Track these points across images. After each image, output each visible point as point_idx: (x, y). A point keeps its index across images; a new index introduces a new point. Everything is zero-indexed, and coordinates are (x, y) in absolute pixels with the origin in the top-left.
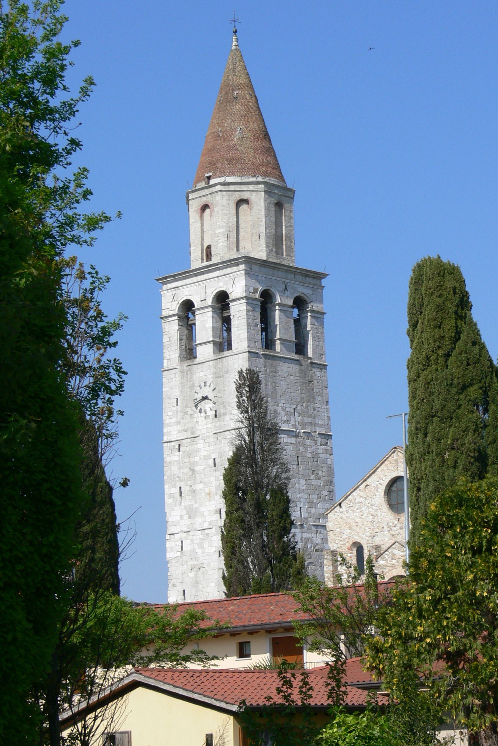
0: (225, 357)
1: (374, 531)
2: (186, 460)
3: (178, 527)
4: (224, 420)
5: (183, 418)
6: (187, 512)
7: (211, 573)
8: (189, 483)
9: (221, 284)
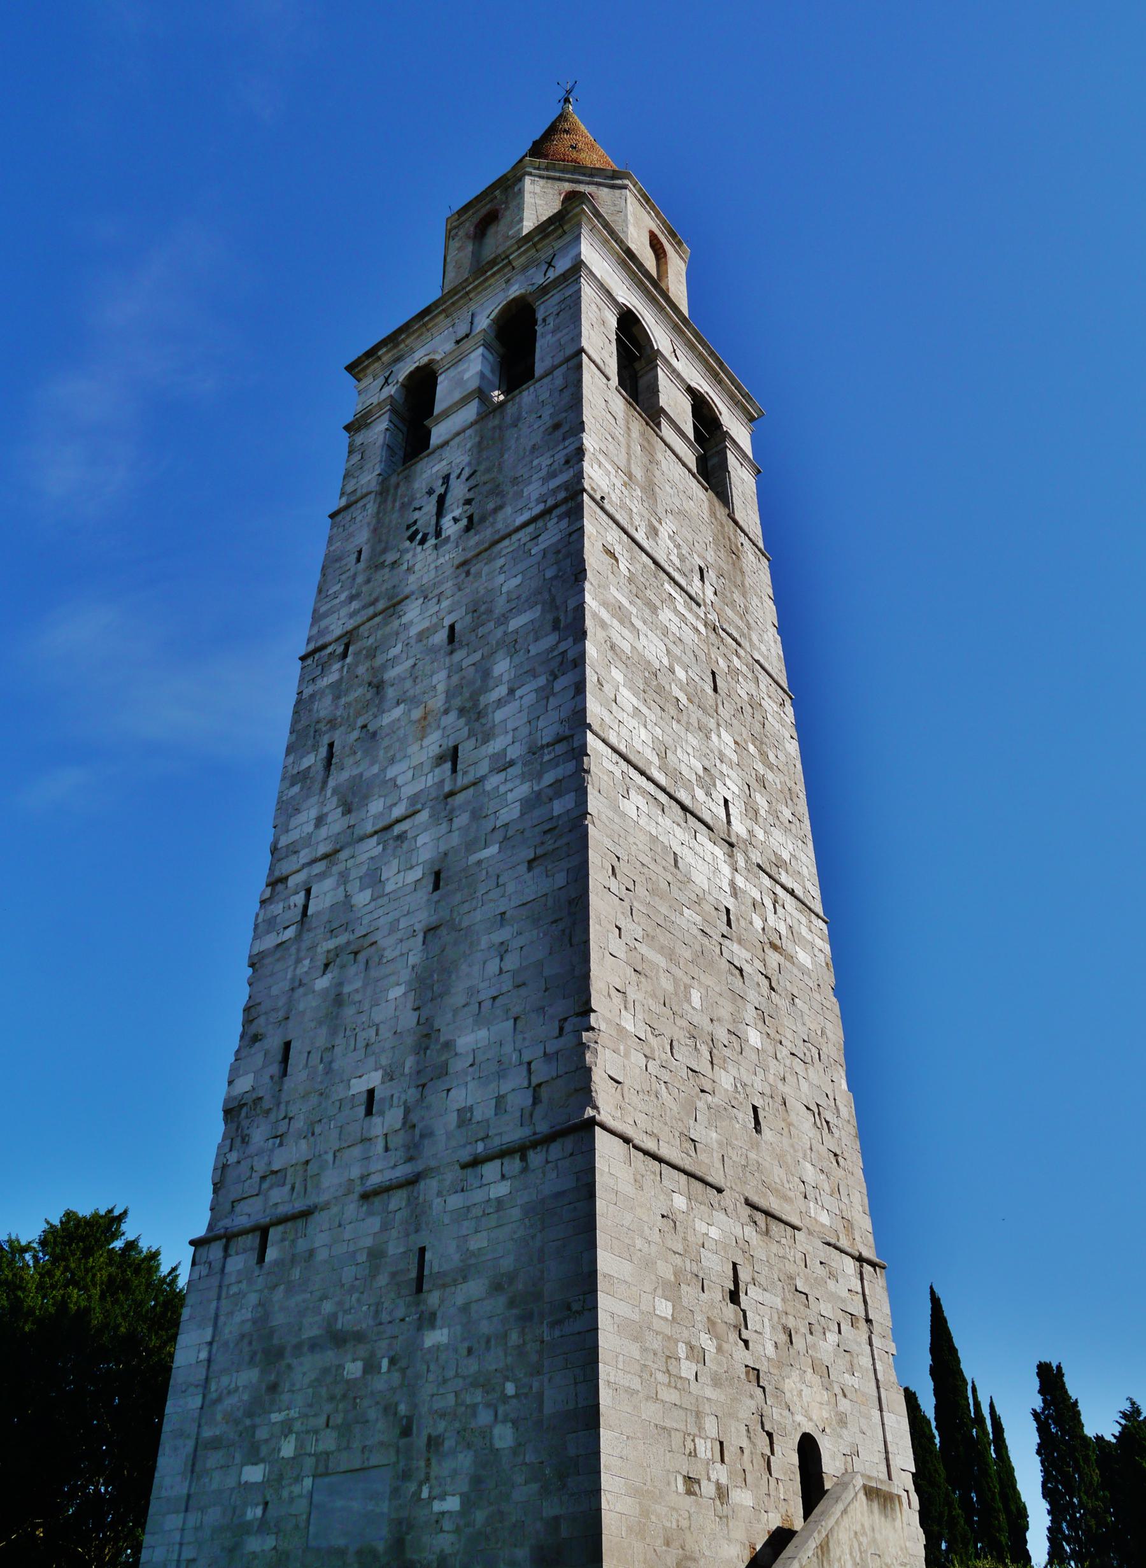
3: (302, 853)
7: (397, 953)
8: (360, 722)
9: (516, 287)
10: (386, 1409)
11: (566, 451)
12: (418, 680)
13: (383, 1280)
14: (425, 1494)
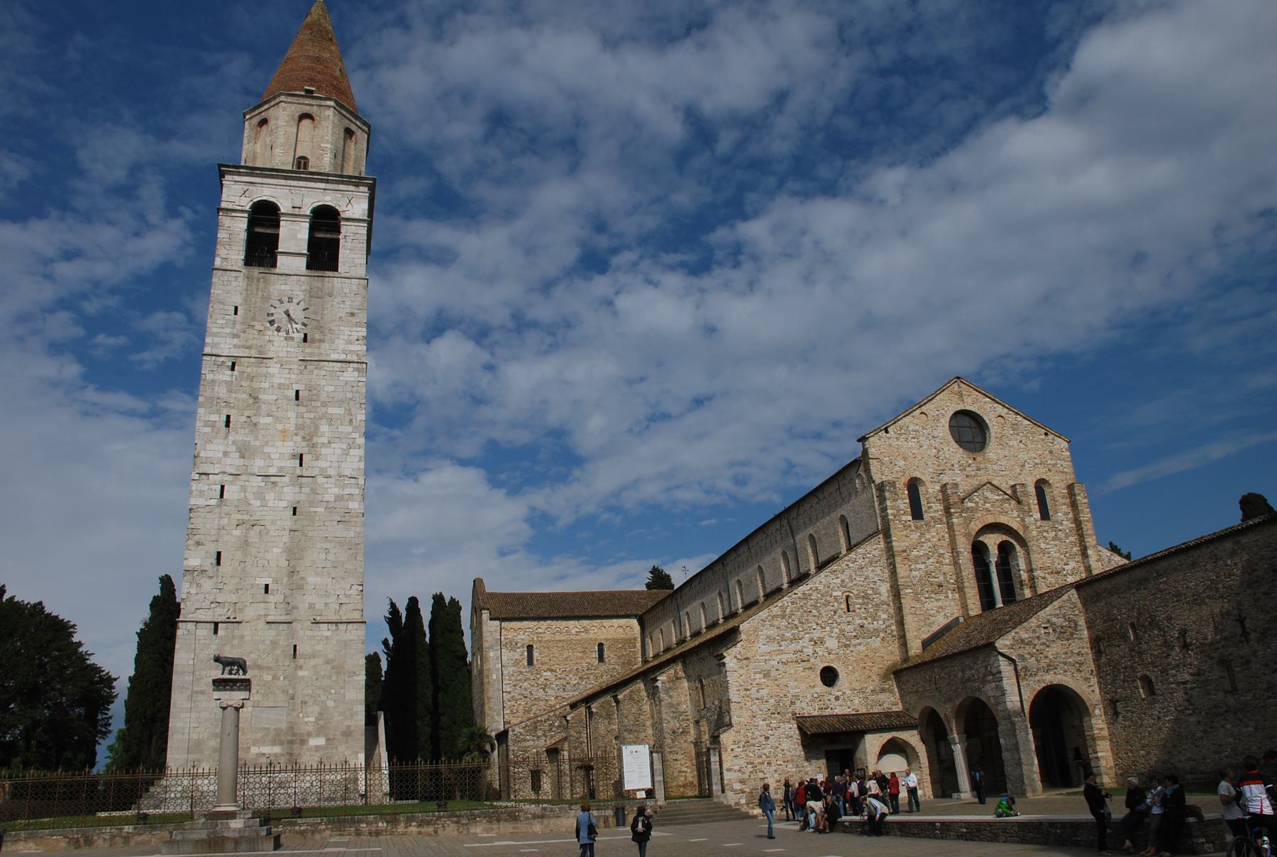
0: (328, 277)
1: (941, 468)
2: (244, 383)
3: (216, 466)
4: (319, 348)
5: (244, 332)
6: (237, 449)
8: (247, 413)
10: (283, 691)
11: (357, 334)
12: (280, 410)
13: (278, 652)
14: (301, 715)
